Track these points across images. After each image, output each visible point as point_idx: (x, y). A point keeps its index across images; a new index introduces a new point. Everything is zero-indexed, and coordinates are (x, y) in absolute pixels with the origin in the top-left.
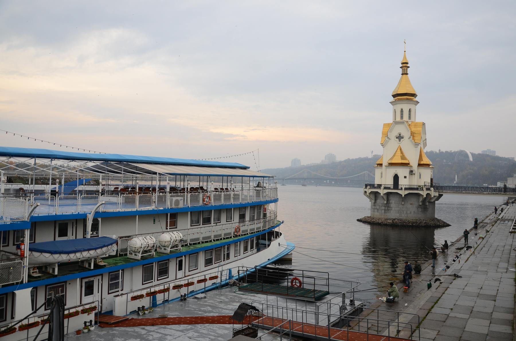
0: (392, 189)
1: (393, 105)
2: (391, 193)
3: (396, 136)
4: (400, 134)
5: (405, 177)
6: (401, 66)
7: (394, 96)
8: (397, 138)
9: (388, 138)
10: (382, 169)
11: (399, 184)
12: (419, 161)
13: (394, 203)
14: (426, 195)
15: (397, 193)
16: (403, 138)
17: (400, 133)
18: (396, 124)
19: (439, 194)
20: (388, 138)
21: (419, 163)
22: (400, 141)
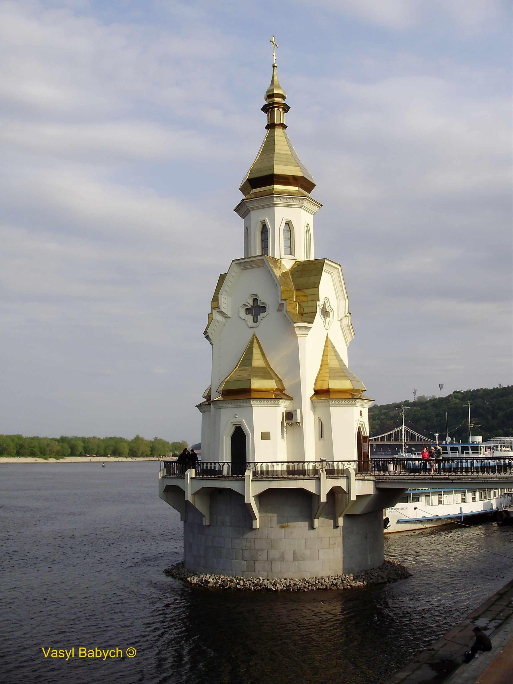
0: (227, 478)
1: (243, 216)
2: (221, 491)
3: (245, 305)
4: (255, 300)
5: (266, 436)
6: (266, 103)
7: (243, 189)
8: (248, 311)
9: (221, 313)
10: (210, 411)
11: (249, 459)
12: (316, 381)
13: (228, 524)
14: (328, 494)
15: (229, 489)
16: (263, 309)
17: (256, 295)
18: (243, 270)
19: (377, 489)
20: (221, 313)
21: (318, 388)
22: (255, 321)
